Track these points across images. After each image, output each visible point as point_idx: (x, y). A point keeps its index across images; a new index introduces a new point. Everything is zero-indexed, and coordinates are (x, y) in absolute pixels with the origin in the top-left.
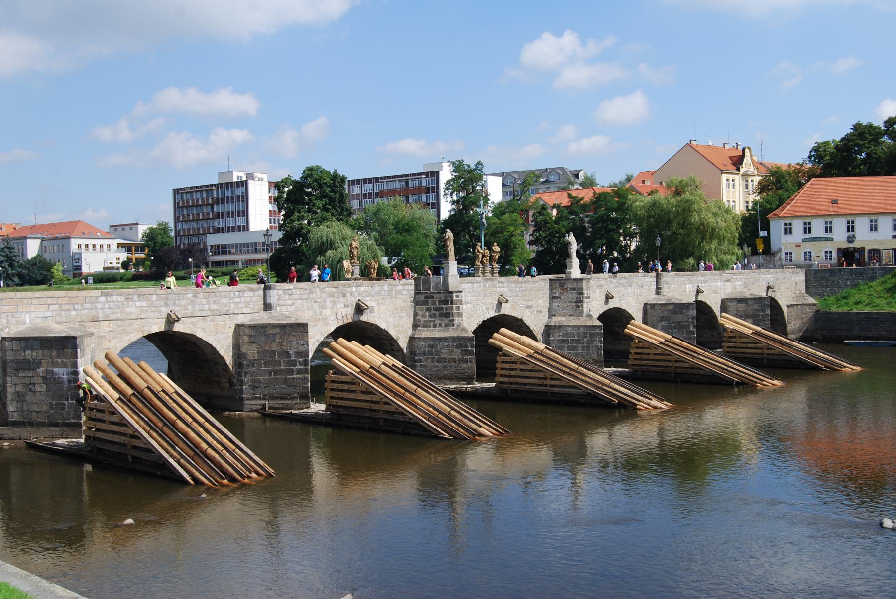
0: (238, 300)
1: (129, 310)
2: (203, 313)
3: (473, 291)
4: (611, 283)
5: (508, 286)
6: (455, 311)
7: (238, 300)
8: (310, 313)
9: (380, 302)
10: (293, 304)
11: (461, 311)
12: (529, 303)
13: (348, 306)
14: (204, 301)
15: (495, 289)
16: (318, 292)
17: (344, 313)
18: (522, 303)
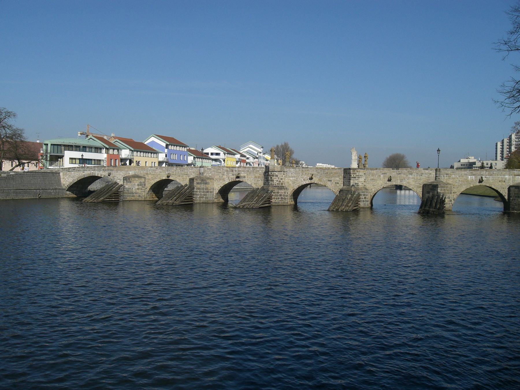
0: (191, 171)
1: (156, 172)
2: (179, 174)
3: (296, 172)
4: (394, 172)
5: (316, 171)
6: (270, 179)
7: (191, 171)
8: (218, 176)
9: (248, 174)
10: (211, 173)
11: (273, 179)
12: (330, 179)
13: (234, 175)
14: (179, 171)
15: (308, 172)
16: (222, 170)
17: (232, 177)
18: (325, 179)
